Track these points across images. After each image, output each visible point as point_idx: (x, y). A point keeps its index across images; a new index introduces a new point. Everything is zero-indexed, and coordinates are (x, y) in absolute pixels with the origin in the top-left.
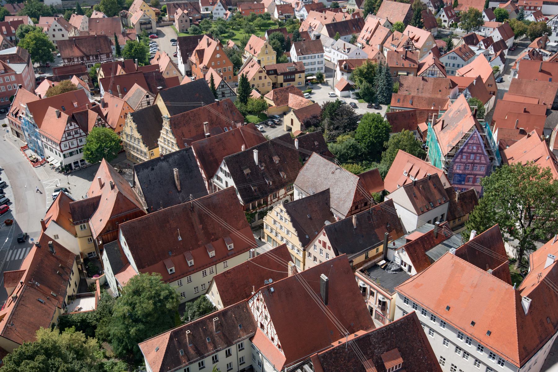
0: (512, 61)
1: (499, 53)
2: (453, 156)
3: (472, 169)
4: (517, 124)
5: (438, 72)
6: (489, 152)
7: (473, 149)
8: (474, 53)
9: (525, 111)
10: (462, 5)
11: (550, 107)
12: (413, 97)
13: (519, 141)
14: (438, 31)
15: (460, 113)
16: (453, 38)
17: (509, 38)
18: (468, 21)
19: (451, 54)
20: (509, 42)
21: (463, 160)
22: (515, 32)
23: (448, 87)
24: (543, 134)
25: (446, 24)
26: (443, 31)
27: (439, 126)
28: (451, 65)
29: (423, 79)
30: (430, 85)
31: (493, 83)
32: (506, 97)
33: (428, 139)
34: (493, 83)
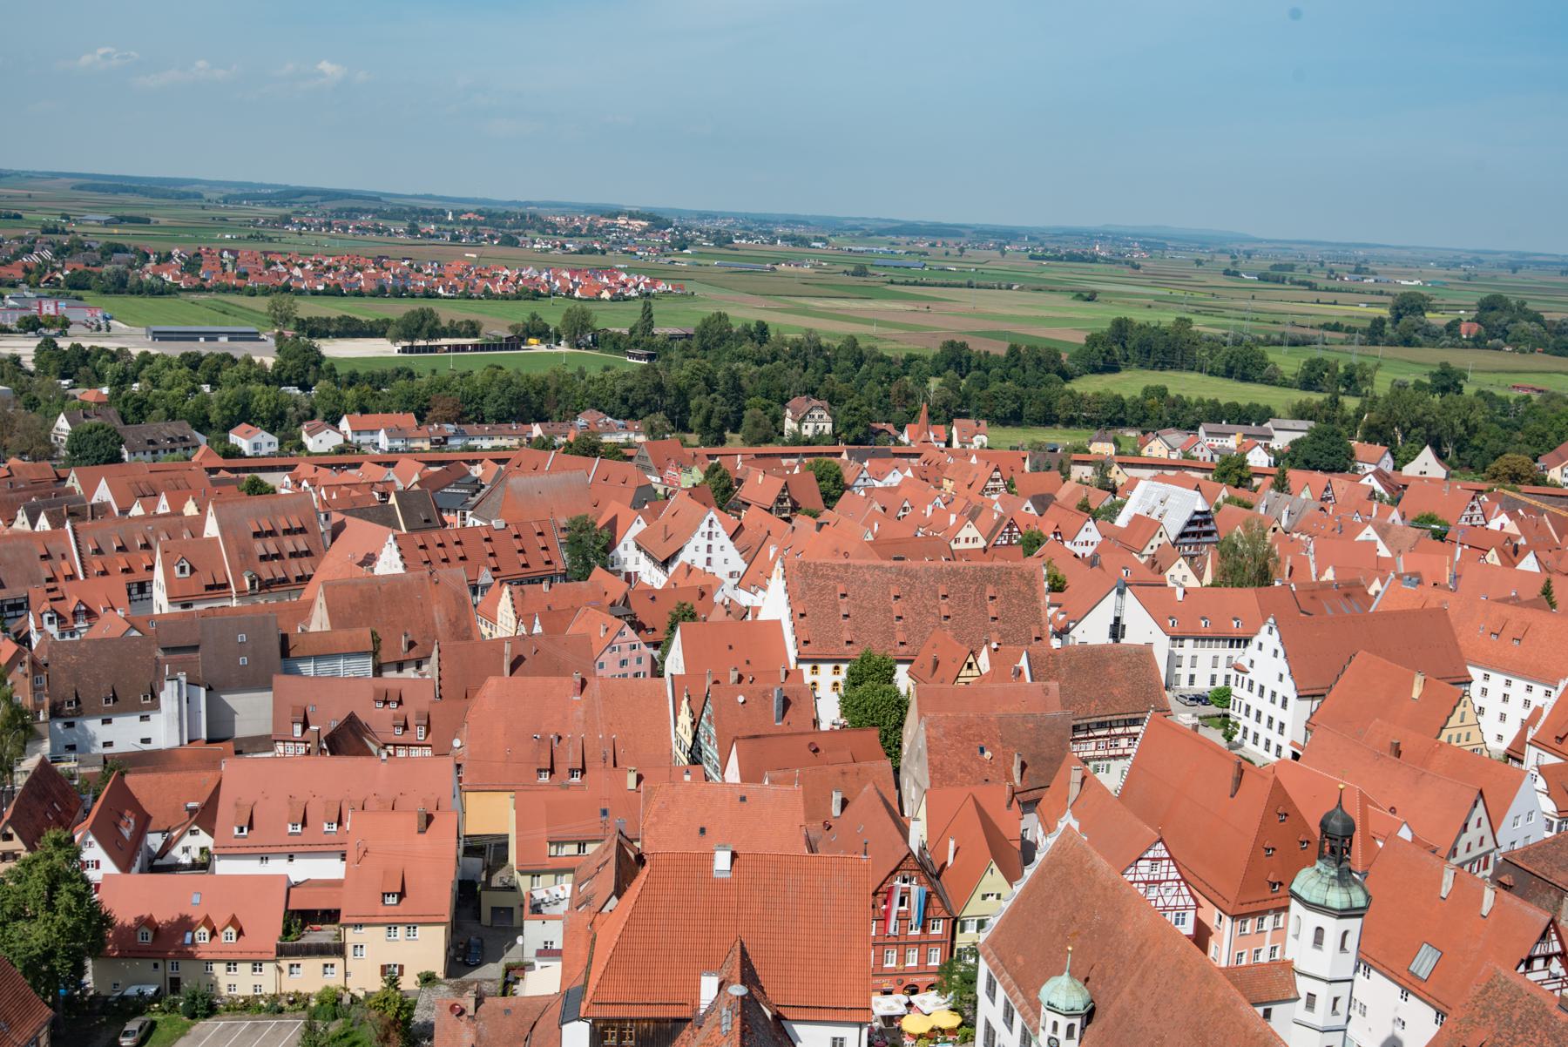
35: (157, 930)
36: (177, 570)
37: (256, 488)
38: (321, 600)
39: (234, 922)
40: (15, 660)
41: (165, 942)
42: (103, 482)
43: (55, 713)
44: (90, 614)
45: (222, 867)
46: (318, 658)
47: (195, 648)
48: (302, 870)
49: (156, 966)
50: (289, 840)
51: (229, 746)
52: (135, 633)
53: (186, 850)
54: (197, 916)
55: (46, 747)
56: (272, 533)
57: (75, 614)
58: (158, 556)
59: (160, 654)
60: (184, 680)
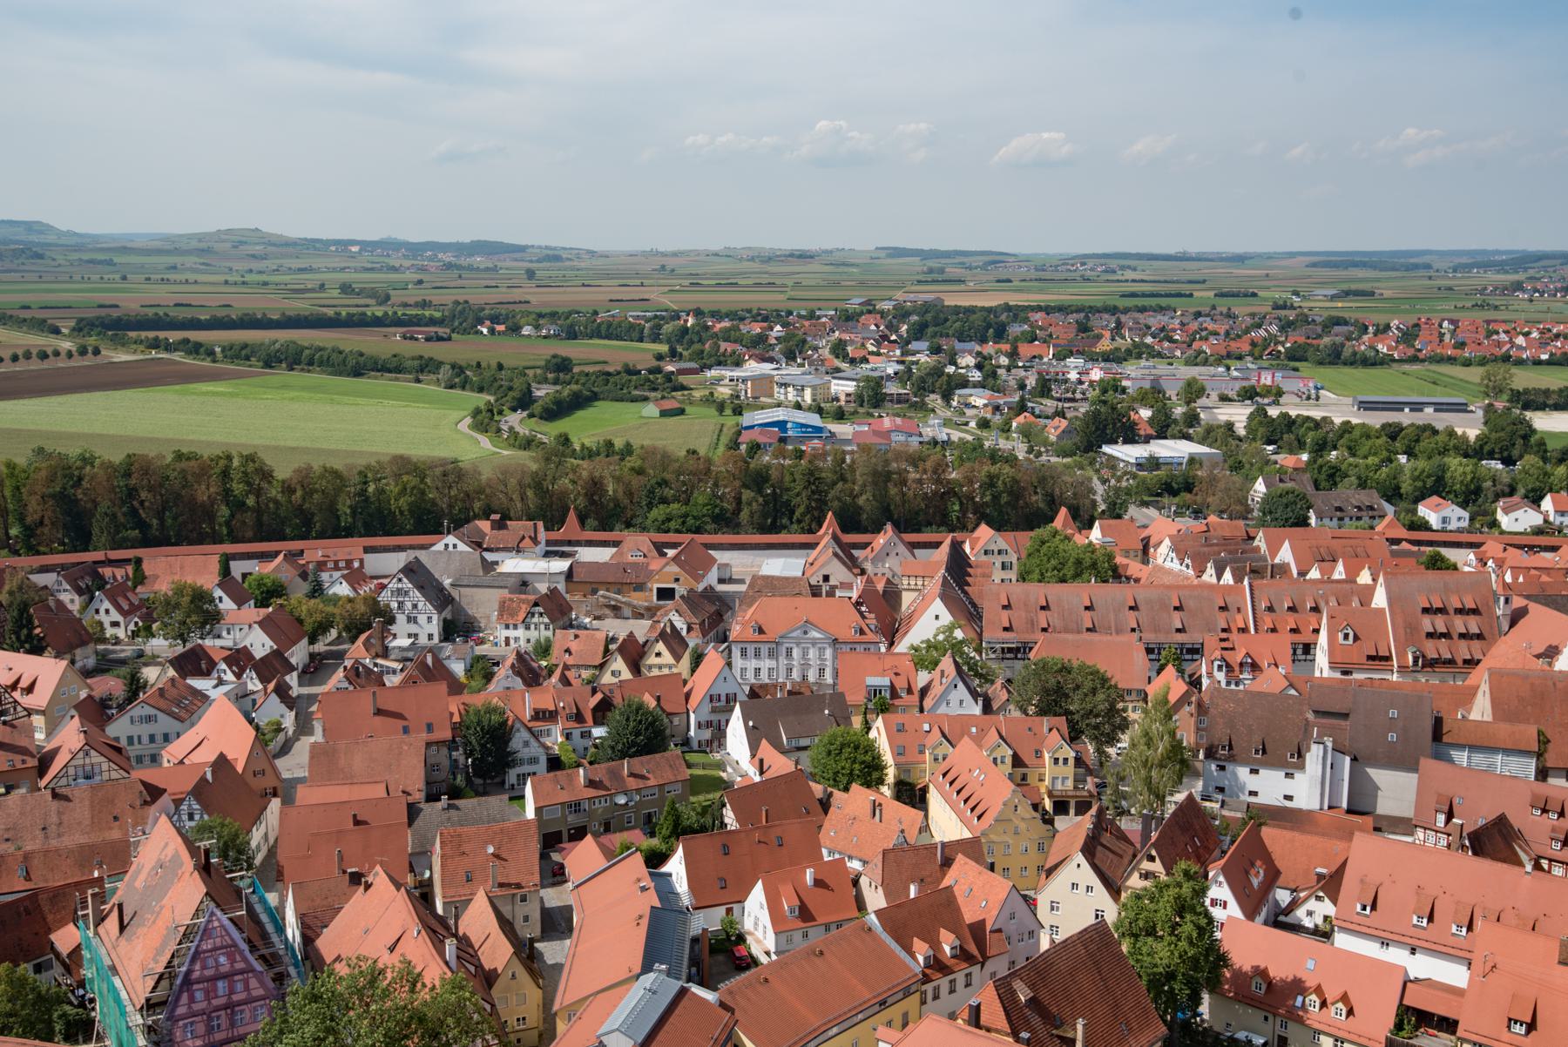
0: (312, 698)
1: (271, 686)
2: (164, 1003)
3: (232, 1025)
4: (341, 858)
5: (105, 766)
6: (270, 960)
7: (218, 965)
8: (207, 697)
9: (357, 822)
10: (156, 577)
11: (419, 796)
12: (27, 857)
13: (347, 907)
14: (97, 653)
15: (165, 868)
16: (146, 665)
17: (295, 643)
18: (178, 615)
19: (137, 710)
20: (298, 654)
21: (196, 1007)
22: (308, 627)
23: (138, 803)
24: (412, 870)
25: (121, 633)
26: (114, 652)
27: (112, 923)
28: (145, 740)
29: (55, 795)
30: (80, 810)
31: (265, 765)
32: (303, 795)
33: (88, 972)
34: (265, 765)
35: (1270, 984)
36: (1341, 636)
37: (1437, 563)
38: (1485, 688)
39: (1345, 998)
40: (1184, 700)
41: (1275, 998)
42: (1287, 544)
43: (1210, 754)
44: (1255, 667)
45: (1342, 940)
46: (1473, 748)
47: (1345, 716)
48: (1422, 966)
49: (1266, 1019)
50: (1413, 932)
51: (1368, 821)
52: (1293, 692)
53: (1310, 913)
54: (1311, 983)
55: (1199, 785)
56: (1441, 611)
57: (1241, 664)
58: (1324, 621)
59: (1310, 716)
60: (1330, 745)
